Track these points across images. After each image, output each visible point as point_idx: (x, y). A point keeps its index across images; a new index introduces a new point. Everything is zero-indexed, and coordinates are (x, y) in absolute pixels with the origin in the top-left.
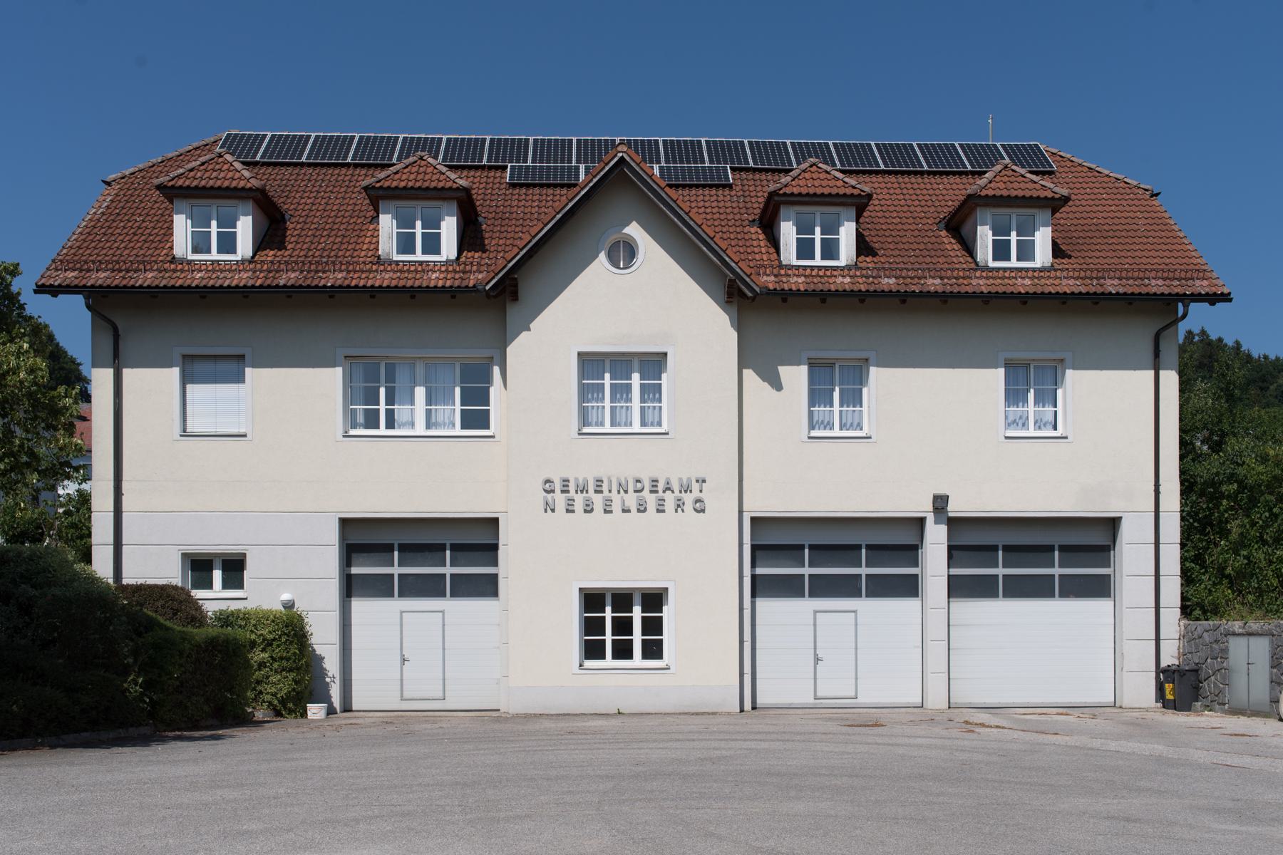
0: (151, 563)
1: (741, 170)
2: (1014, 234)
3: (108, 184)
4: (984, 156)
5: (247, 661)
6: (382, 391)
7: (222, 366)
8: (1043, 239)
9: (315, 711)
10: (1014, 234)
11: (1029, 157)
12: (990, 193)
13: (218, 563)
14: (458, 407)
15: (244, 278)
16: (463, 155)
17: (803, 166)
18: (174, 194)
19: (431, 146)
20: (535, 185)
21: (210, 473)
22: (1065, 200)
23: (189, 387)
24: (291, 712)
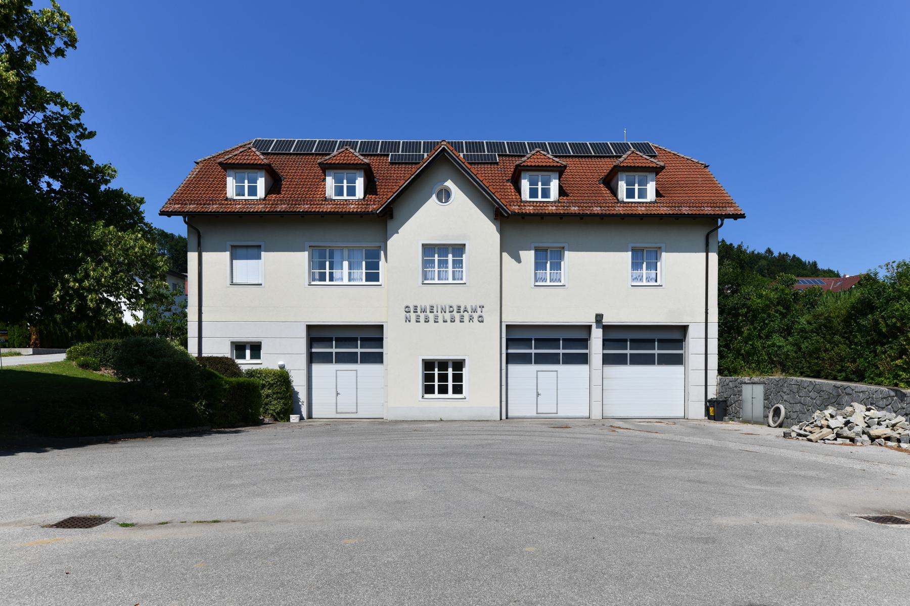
0: (217, 347)
1: (503, 155)
2: (636, 185)
3: (197, 163)
4: (622, 148)
5: (260, 394)
6: (327, 263)
7: (252, 251)
8: (651, 188)
9: (294, 418)
10: (636, 185)
11: (645, 148)
12: (625, 165)
13: (248, 346)
14: (364, 271)
15: (260, 208)
16: (368, 148)
17: (533, 152)
18: (227, 167)
19: (353, 145)
20: (402, 163)
21: (245, 303)
22: (663, 168)
23: (234, 261)
24: (282, 419)
